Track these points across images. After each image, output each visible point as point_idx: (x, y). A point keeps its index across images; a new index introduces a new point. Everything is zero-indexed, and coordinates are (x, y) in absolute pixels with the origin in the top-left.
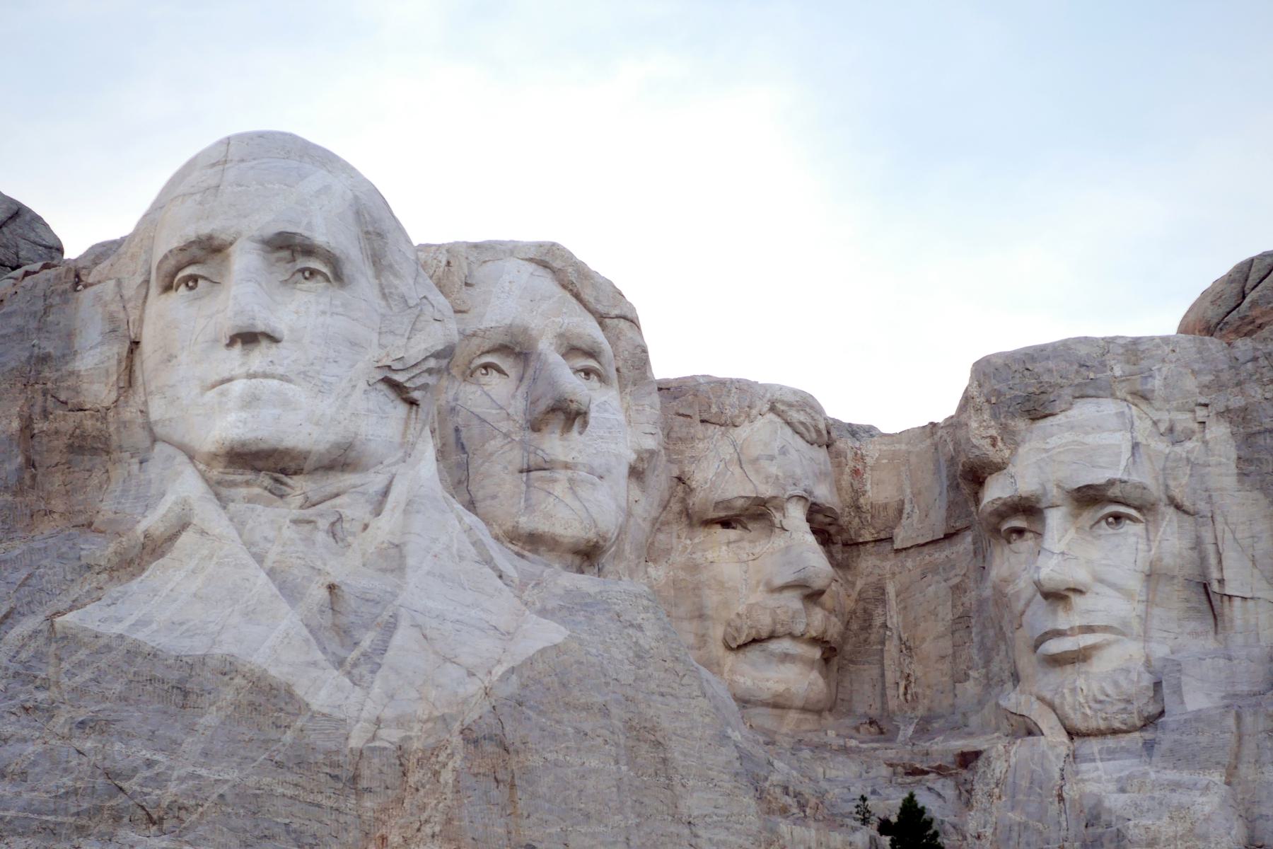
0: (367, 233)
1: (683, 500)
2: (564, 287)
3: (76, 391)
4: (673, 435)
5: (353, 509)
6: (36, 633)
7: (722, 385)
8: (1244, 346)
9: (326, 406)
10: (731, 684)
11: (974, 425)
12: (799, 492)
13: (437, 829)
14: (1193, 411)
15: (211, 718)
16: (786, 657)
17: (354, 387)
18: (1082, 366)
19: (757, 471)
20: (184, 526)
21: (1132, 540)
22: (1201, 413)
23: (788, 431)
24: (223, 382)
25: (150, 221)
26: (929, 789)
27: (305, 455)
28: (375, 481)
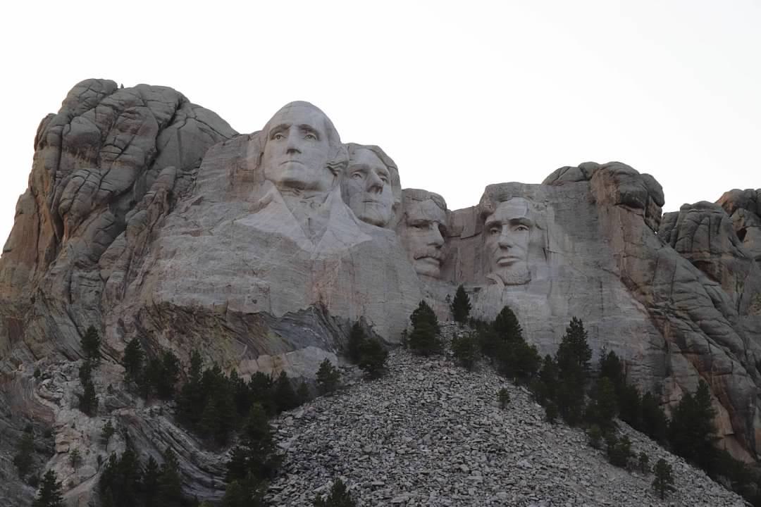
3: (246, 165)
5: (317, 200)
6: (227, 225)
7: (418, 191)
8: (558, 188)
9: (312, 172)
10: (415, 268)
15: (274, 249)
16: (429, 263)
18: (515, 189)
20: (271, 201)
22: (546, 203)
23: (435, 204)
24: (285, 163)
25: (267, 126)
27: (305, 184)
28: (324, 194)
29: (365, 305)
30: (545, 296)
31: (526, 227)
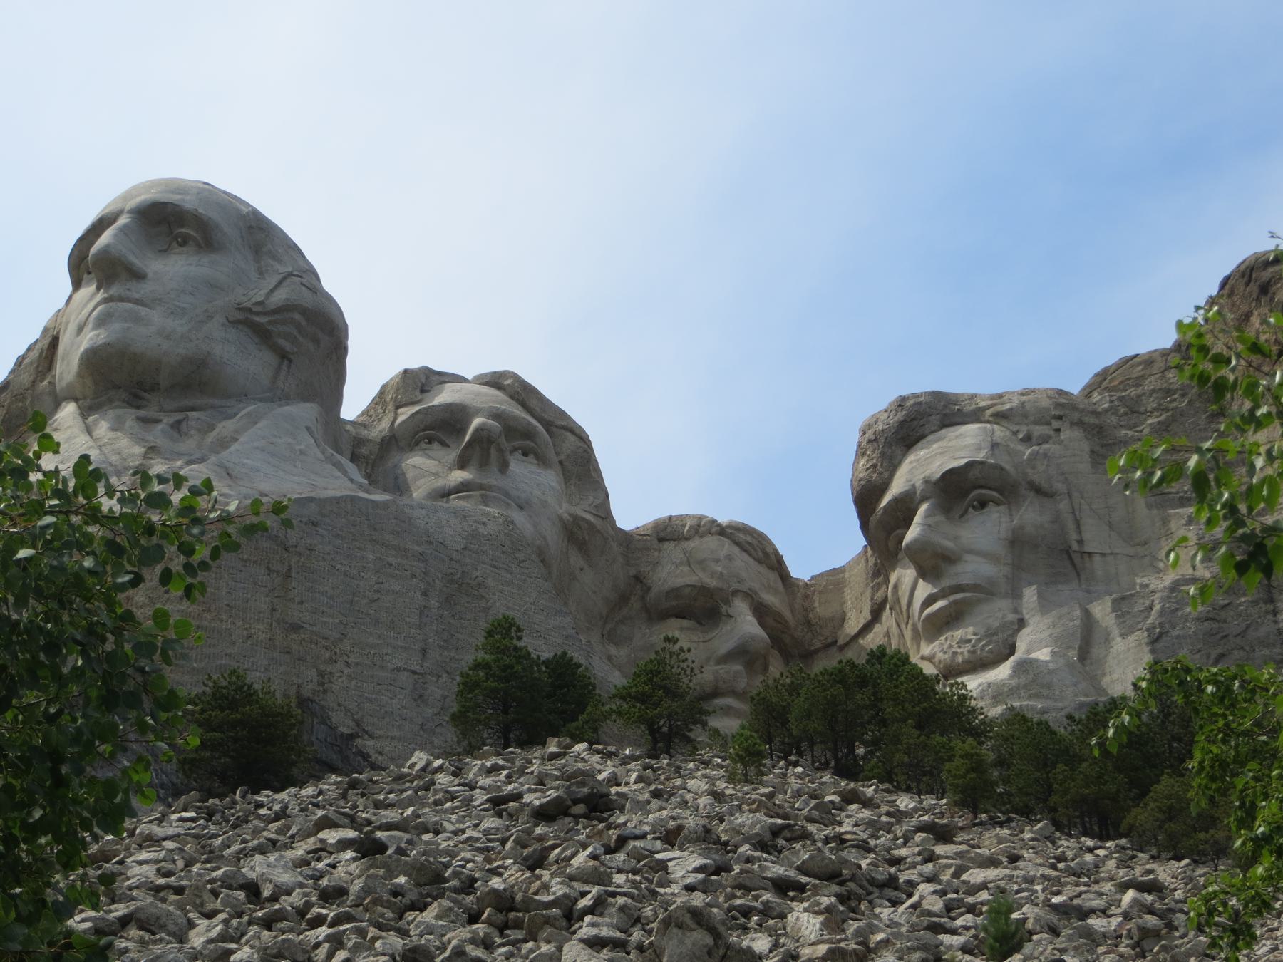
0: (250, 227)
1: (643, 598)
2: (512, 397)
9: (178, 325)
12: (744, 587)
14: (1049, 424)
16: (727, 711)
17: (210, 317)
19: (704, 570)
21: (995, 516)
22: (1056, 424)
23: (736, 550)
29: (322, 667)
31: (994, 493)
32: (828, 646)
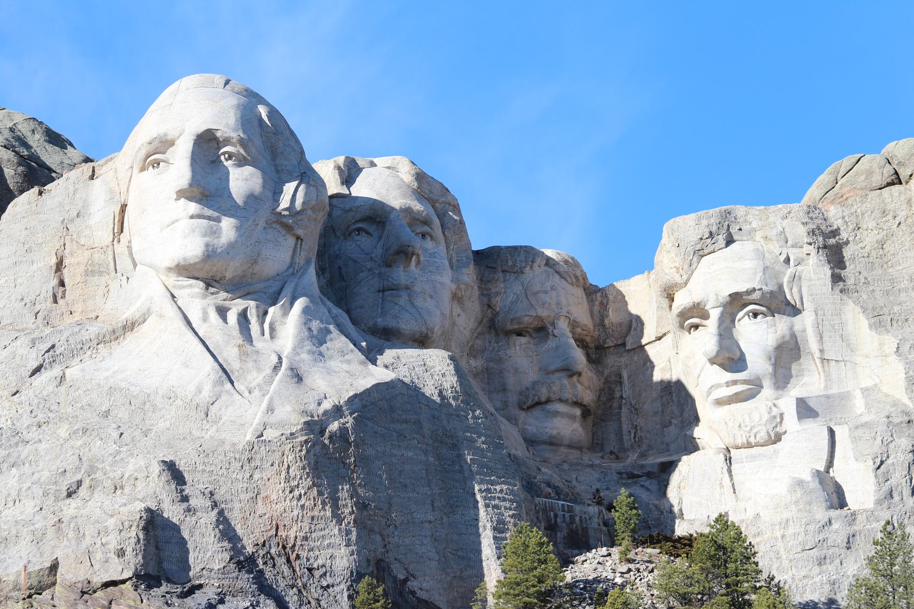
4: (485, 279)
11: (666, 261)
13: (303, 492)
16: (556, 414)
26: (642, 486)
30: (822, 468)
31: (764, 309)
32: (616, 346)
